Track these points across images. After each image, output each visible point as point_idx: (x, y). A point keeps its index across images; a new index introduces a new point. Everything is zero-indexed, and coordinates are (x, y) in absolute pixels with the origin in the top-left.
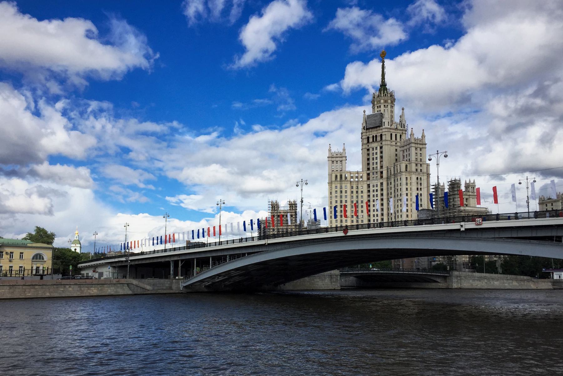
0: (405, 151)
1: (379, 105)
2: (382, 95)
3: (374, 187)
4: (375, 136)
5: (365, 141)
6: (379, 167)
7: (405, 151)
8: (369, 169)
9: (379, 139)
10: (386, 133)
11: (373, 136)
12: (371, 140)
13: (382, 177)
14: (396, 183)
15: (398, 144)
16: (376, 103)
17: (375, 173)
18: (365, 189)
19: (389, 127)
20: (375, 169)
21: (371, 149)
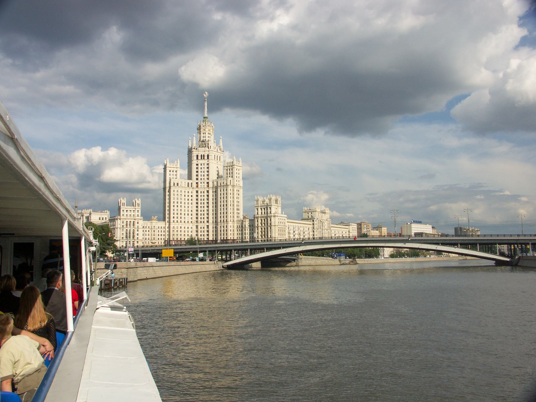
0: (228, 170)
1: (204, 132)
2: (207, 125)
3: (201, 192)
4: (203, 155)
5: (195, 158)
6: (206, 179)
7: (228, 170)
8: (197, 179)
9: (206, 157)
10: (212, 154)
11: (201, 155)
12: (199, 158)
13: (208, 186)
14: (222, 192)
15: (219, 163)
16: (202, 130)
17: (202, 183)
18: (195, 194)
19: (214, 150)
20: (203, 179)
21: (199, 165)
